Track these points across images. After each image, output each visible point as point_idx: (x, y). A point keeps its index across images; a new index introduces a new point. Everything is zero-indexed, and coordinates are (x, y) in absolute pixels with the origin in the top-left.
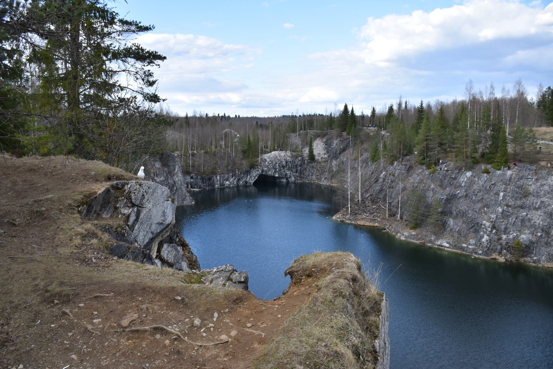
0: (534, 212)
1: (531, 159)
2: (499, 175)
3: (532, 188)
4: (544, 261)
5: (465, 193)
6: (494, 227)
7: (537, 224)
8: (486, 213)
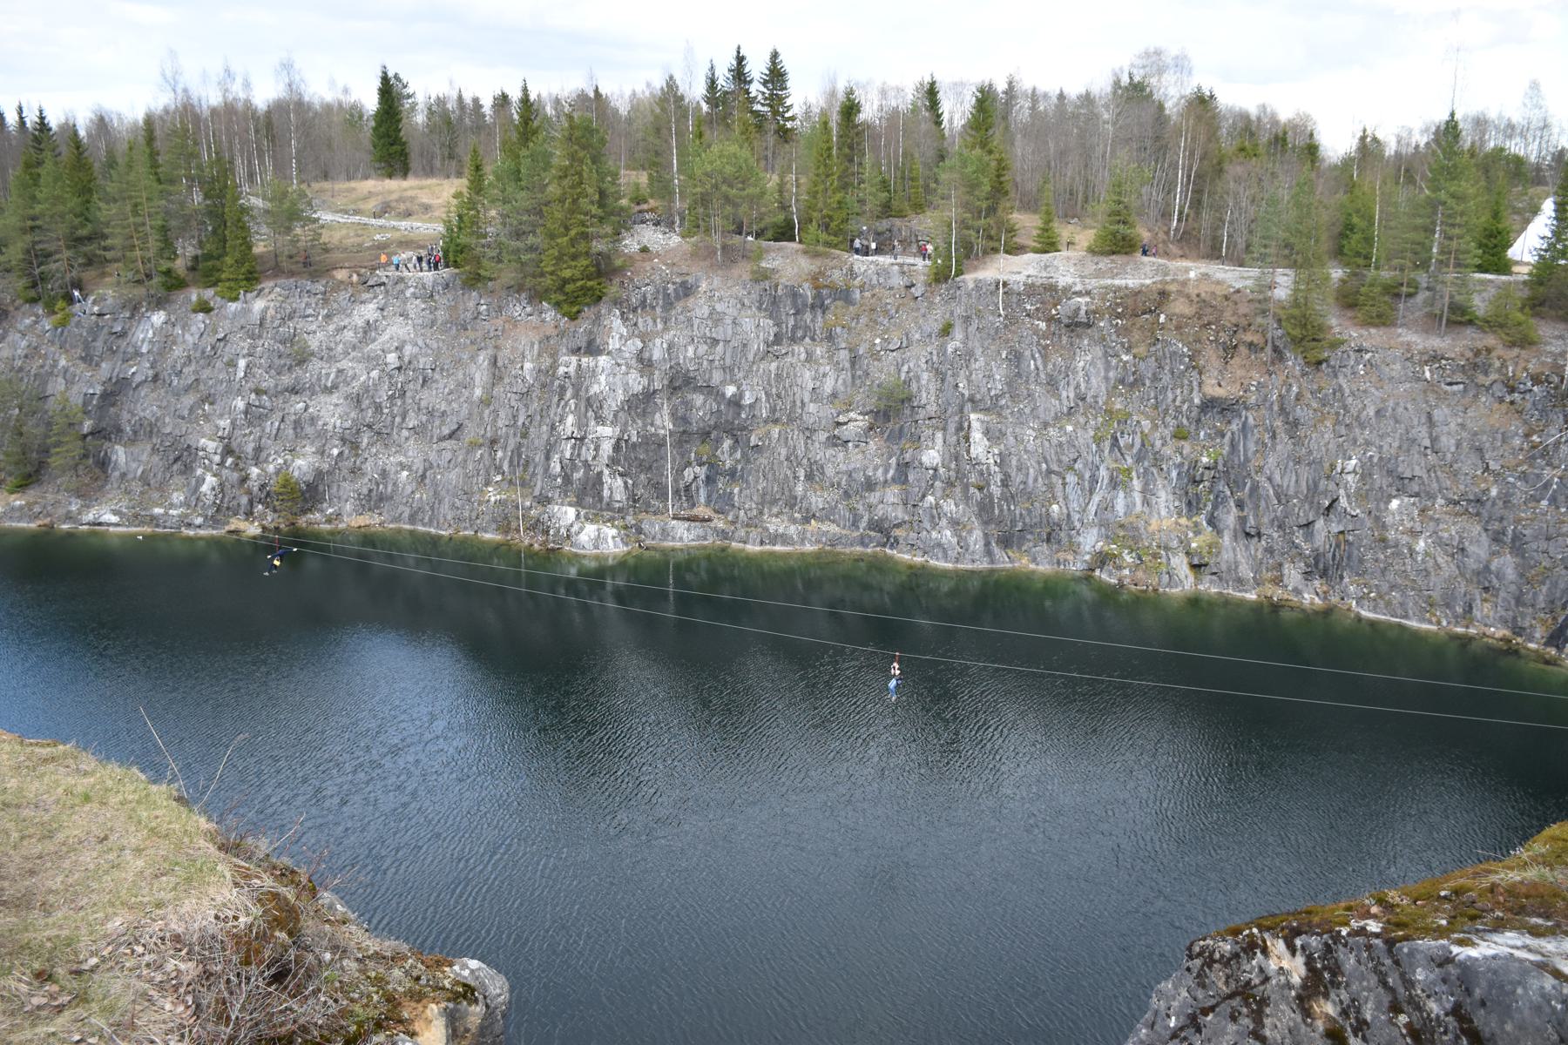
0: (323, 398)
1: (309, 265)
2: (235, 315)
3: (314, 343)
4: (350, 515)
5: (151, 373)
6: (228, 451)
7: (330, 427)
8: (207, 417)
